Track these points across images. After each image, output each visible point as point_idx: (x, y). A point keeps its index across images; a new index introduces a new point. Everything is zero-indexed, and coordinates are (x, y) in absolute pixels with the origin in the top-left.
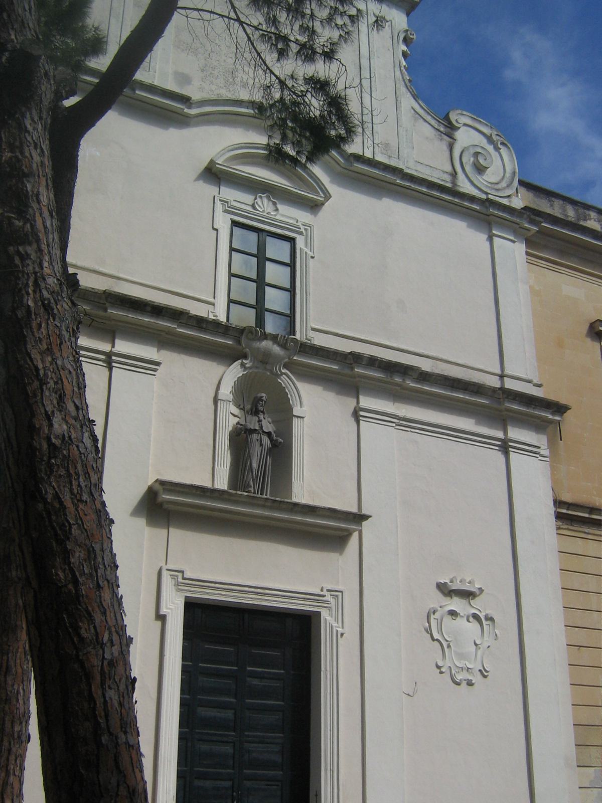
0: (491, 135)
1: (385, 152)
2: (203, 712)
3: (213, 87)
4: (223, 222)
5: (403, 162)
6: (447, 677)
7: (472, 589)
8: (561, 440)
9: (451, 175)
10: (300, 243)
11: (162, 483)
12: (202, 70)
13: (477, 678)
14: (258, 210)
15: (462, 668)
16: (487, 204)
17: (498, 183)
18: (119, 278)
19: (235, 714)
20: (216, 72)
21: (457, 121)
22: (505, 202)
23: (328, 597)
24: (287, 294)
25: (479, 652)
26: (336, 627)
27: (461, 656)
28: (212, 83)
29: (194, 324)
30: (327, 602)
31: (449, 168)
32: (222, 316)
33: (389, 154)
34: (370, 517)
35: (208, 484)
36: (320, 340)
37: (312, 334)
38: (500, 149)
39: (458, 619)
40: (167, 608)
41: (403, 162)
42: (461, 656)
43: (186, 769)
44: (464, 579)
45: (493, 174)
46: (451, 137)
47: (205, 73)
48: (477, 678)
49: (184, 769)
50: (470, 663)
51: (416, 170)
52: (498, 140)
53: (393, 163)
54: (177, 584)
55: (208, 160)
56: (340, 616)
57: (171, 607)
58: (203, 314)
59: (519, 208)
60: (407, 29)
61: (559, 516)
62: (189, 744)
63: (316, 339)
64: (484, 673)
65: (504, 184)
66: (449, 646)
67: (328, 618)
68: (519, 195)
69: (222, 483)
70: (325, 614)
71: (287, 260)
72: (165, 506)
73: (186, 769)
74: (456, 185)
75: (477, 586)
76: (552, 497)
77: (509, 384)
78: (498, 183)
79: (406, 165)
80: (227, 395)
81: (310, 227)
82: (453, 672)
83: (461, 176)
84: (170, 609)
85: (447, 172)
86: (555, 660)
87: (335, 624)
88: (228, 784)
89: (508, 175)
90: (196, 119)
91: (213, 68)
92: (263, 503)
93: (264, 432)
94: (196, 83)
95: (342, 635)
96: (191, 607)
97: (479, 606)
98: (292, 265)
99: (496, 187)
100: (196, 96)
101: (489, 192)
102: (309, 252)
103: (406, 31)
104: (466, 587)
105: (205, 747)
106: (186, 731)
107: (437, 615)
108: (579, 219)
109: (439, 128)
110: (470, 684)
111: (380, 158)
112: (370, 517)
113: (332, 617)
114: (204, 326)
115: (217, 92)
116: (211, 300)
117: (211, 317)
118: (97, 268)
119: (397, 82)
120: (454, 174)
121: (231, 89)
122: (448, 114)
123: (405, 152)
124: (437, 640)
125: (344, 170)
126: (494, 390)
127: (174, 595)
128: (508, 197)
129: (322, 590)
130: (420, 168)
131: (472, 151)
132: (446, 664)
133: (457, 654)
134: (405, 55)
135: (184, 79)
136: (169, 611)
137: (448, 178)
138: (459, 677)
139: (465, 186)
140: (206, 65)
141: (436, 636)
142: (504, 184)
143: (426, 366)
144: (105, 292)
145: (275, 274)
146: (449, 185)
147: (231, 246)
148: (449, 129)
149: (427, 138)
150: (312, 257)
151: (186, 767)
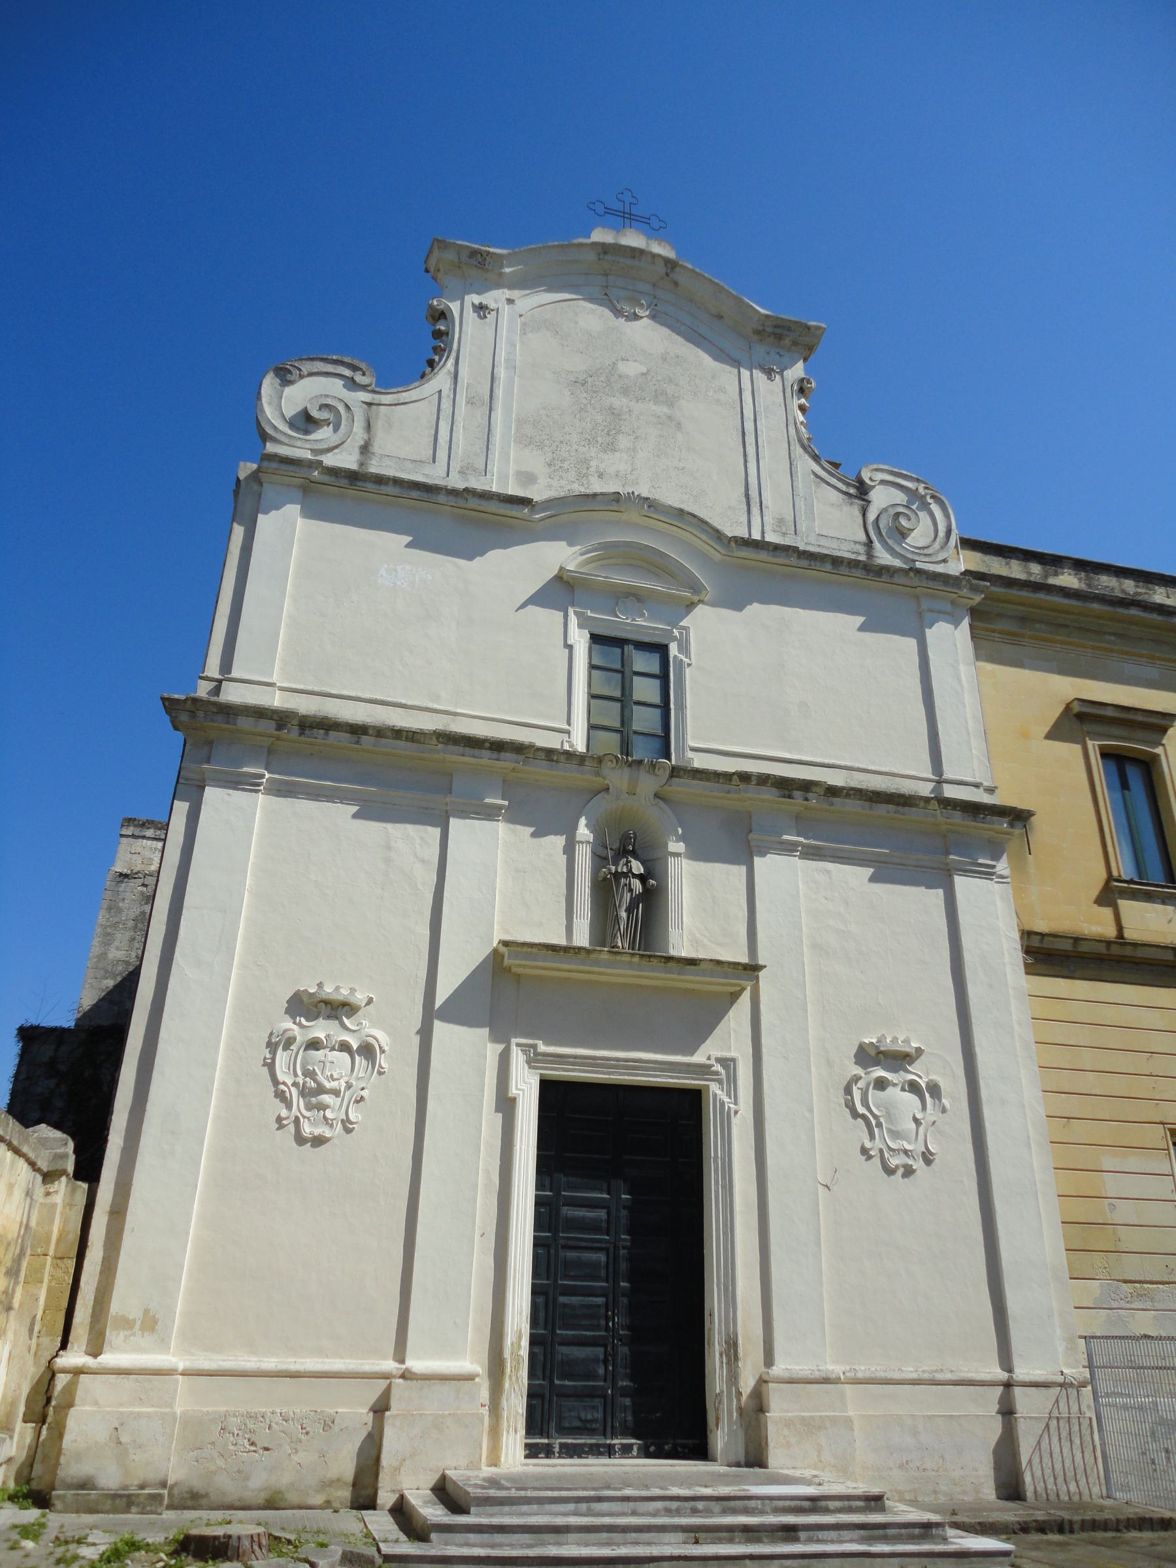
0: (917, 489)
1: (778, 529)
2: (568, 1212)
3: (563, 483)
4: (580, 640)
5: (802, 538)
6: (877, 1161)
7: (908, 1050)
8: (1030, 854)
9: (865, 544)
10: (673, 649)
11: (506, 944)
12: (549, 465)
13: (918, 1164)
14: (620, 618)
15: (898, 1150)
16: (912, 574)
17: (929, 547)
18: (456, 714)
19: (608, 1214)
20: (566, 465)
21: (871, 479)
22: (940, 569)
23: (718, 1068)
24: (617, 706)
25: (921, 1129)
26: (728, 1103)
27: (896, 1135)
28: (561, 477)
29: (543, 758)
30: (717, 1073)
31: (863, 538)
32: (580, 743)
33: (784, 530)
34: (765, 967)
35: (562, 941)
36: (699, 762)
37: (690, 754)
38: (930, 504)
39: (890, 1089)
40: (517, 1089)
41: (802, 538)
42: (896, 1135)
43: (548, 1282)
44: (897, 1038)
45: (922, 536)
46: (864, 500)
47: (553, 468)
48: (918, 1164)
49: (546, 1282)
50: (909, 1143)
51: (819, 546)
52: (926, 494)
53: (788, 541)
54: (529, 1062)
55: (558, 568)
56: (733, 1091)
57: (523, 1087)
58: (555, 745)
59: (957, 574)
60: (804, 376)
61: (1028, 951)
62: (552, 1251)
63: (695, 760)
64: (928, 1158)
65: (937, 545)
66: (879, 1125)
67: (719, 1092)
68: (961, 556)
69: (582, 938)
70: (714, 1087)
71: (618, 666)
72: (514, 970)
73: (548, 1282)
74: (872, 556)
75: (914, 1045)
76: (1016, 927)
77: (950, 792)
78: (929, 547)
79: (805, 541)
80: (587, 835)
81: (686, 630)
82: (886, 1155)
83: (877, 545)
84: (520, 1090)
85: (859, 543)
86: (1029, 1137)
87: (726, 1100)
88: (600, 1300)
89: (941, 534)
90: (541, 523)
91: (563, 461)
92: (629, 959)
93: (633, 874)
94: (542, 481)
95: (736, 1112)
96: (548, 1088)
97: (919, 1072)
98: (664, 677)
99: (926, 551)
100: (536, 498)
101: (916, 559)
102: (684, 659)
103: (802, 380)
104: (900, 1047)
105: (572, 1255)
106: (547, 1236)
107: (861, 1084)
108: (1046, 577)
109: (847, 491)
110: (909, 1172)
111: (771, 538)
112: (765, 967)
113: (723, 1091)
114: (555, 758)
115: (569, 487)
116: (566, 727)
117: (567, 747)
118: (430, 705)
119: (792, 443)
120: (869, 543)
121: (585, 482)
122: (860, 471)
123: (803, 526)
124: (863, 1117)
125: (725, 557)
126: (927, 800)
127: (526, 1073)
128: (945, 561)
129: (709, 1058)
130: (823, 542)
131: (892, 511)
132: (874, 1146)
133: (890, 1131)
134: (802, 408)
135: (528, 478)
136: (521, 1092)
137: (861, 549)
138: (894, 1162)
139: (883, 557)
140: (554, 458)
141: (861, 1110)
142: (937, 545)
143: (836, 779)
144: (434, 732)
145: (645, 690)
146: (862, 558)
147: (590, 663)
148: (862, 491)
149: (833, 505)
150: (689, 665)
151: (548, 1279)
